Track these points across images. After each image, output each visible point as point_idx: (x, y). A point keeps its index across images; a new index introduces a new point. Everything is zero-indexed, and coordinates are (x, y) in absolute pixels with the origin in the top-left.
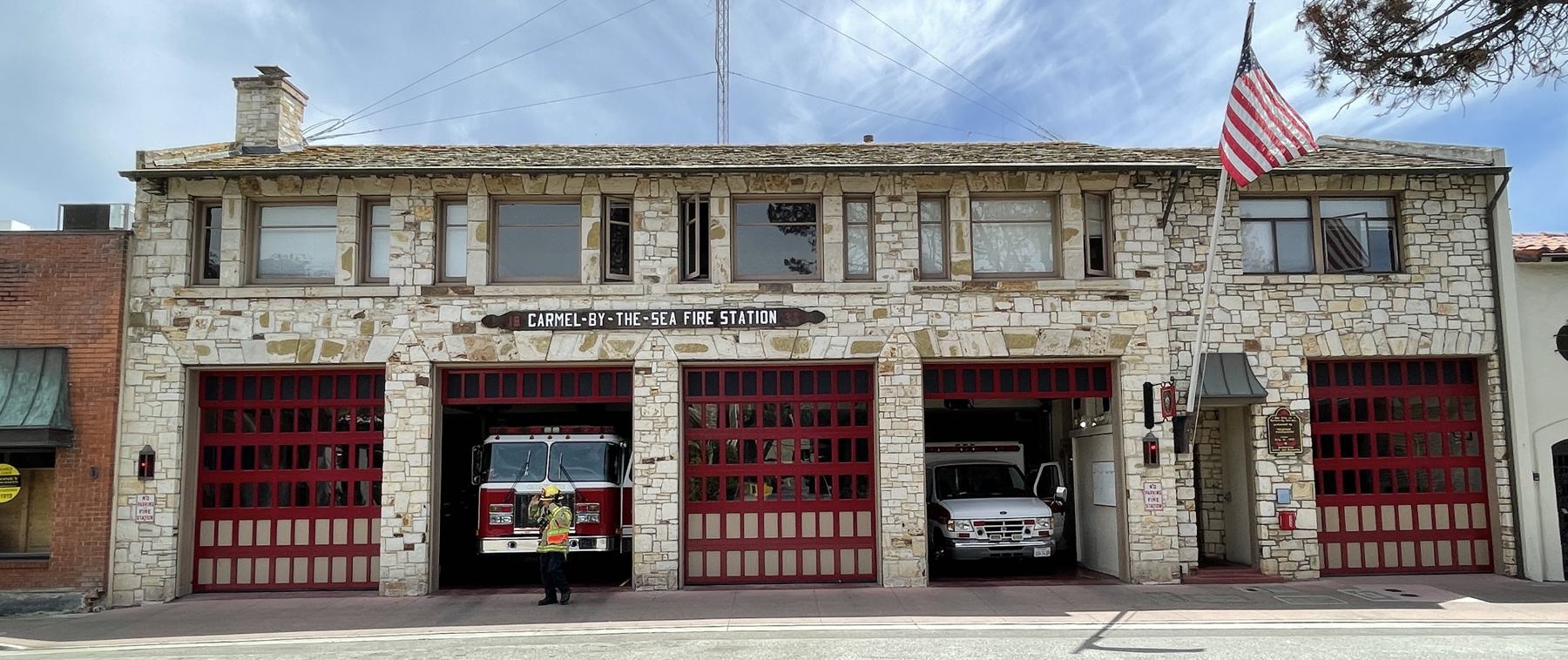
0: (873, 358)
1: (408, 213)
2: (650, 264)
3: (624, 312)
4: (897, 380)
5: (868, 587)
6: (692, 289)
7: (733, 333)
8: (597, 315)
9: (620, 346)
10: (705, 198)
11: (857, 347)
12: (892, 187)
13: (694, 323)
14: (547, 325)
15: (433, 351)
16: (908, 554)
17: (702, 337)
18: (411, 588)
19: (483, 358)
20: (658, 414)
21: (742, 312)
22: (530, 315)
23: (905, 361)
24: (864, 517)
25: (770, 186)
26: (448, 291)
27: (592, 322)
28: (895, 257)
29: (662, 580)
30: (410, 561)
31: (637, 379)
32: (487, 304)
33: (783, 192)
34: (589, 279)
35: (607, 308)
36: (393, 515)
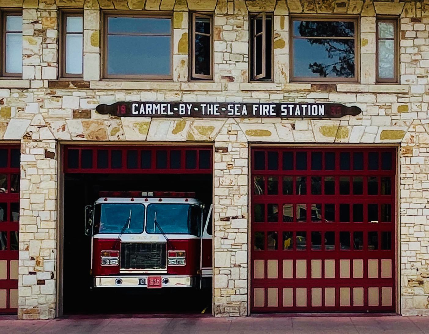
0: (398, 143)
1: (37, 22)
2: (227, 67)
3: (207, 104)
4: (414, 160)
5: (390, 316)
6: (260, 87)
7: (291, 122)
8: (186, 106)
9: (203, 130)
10: (270, 16)
11: (384, 134)
12: (414, 11)
13: (261, 114)
14: (147, 113)
15: (58, 132)
16: (420, 291)
17: (267, 125)
18: (42, 314)
19: (97, 137)
20: (233, 184)
21: (298, 106)
22: (134, 105)
23: (422, 146)
24: (387, 264)
25: (320, 8)
26: (69, 84)
27: (182, 110)
28: (415, 66)
29: (235, 309)
30: (42, 293)
31: (217, 156)
32: (99, 96)
33: (330, 13)
34: (179, 77)
35: (194, 100)
36: (28, 258)
